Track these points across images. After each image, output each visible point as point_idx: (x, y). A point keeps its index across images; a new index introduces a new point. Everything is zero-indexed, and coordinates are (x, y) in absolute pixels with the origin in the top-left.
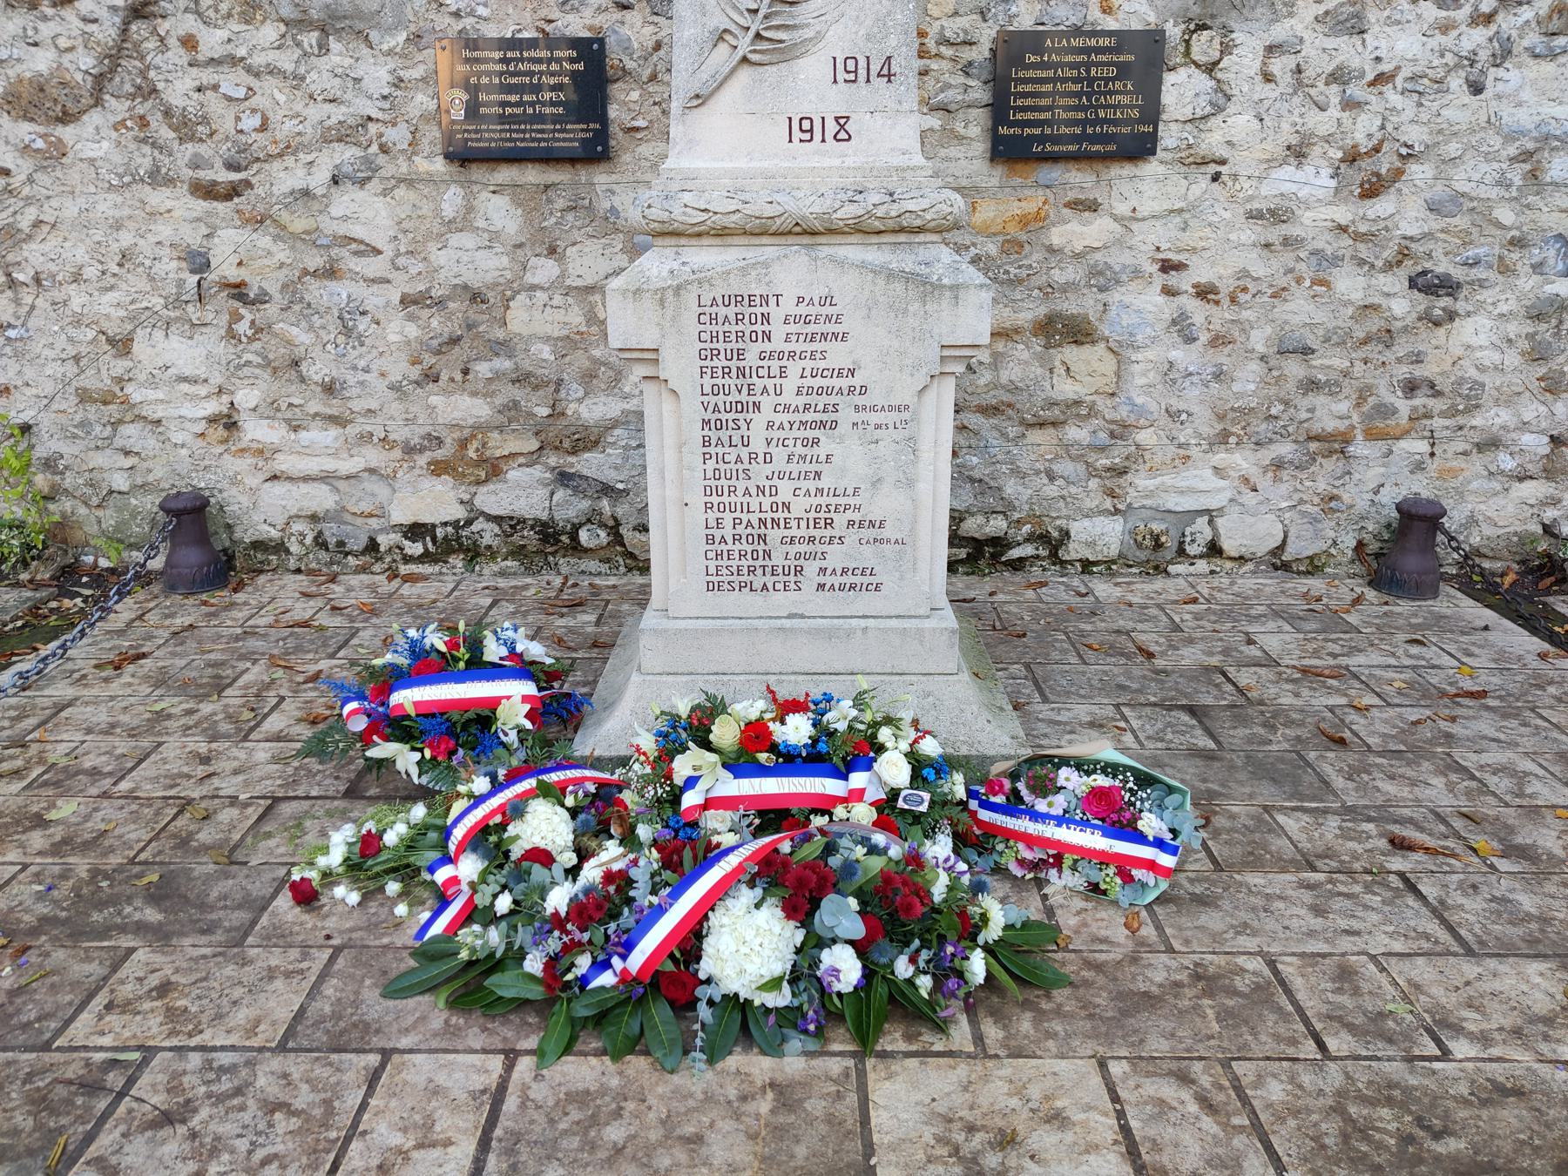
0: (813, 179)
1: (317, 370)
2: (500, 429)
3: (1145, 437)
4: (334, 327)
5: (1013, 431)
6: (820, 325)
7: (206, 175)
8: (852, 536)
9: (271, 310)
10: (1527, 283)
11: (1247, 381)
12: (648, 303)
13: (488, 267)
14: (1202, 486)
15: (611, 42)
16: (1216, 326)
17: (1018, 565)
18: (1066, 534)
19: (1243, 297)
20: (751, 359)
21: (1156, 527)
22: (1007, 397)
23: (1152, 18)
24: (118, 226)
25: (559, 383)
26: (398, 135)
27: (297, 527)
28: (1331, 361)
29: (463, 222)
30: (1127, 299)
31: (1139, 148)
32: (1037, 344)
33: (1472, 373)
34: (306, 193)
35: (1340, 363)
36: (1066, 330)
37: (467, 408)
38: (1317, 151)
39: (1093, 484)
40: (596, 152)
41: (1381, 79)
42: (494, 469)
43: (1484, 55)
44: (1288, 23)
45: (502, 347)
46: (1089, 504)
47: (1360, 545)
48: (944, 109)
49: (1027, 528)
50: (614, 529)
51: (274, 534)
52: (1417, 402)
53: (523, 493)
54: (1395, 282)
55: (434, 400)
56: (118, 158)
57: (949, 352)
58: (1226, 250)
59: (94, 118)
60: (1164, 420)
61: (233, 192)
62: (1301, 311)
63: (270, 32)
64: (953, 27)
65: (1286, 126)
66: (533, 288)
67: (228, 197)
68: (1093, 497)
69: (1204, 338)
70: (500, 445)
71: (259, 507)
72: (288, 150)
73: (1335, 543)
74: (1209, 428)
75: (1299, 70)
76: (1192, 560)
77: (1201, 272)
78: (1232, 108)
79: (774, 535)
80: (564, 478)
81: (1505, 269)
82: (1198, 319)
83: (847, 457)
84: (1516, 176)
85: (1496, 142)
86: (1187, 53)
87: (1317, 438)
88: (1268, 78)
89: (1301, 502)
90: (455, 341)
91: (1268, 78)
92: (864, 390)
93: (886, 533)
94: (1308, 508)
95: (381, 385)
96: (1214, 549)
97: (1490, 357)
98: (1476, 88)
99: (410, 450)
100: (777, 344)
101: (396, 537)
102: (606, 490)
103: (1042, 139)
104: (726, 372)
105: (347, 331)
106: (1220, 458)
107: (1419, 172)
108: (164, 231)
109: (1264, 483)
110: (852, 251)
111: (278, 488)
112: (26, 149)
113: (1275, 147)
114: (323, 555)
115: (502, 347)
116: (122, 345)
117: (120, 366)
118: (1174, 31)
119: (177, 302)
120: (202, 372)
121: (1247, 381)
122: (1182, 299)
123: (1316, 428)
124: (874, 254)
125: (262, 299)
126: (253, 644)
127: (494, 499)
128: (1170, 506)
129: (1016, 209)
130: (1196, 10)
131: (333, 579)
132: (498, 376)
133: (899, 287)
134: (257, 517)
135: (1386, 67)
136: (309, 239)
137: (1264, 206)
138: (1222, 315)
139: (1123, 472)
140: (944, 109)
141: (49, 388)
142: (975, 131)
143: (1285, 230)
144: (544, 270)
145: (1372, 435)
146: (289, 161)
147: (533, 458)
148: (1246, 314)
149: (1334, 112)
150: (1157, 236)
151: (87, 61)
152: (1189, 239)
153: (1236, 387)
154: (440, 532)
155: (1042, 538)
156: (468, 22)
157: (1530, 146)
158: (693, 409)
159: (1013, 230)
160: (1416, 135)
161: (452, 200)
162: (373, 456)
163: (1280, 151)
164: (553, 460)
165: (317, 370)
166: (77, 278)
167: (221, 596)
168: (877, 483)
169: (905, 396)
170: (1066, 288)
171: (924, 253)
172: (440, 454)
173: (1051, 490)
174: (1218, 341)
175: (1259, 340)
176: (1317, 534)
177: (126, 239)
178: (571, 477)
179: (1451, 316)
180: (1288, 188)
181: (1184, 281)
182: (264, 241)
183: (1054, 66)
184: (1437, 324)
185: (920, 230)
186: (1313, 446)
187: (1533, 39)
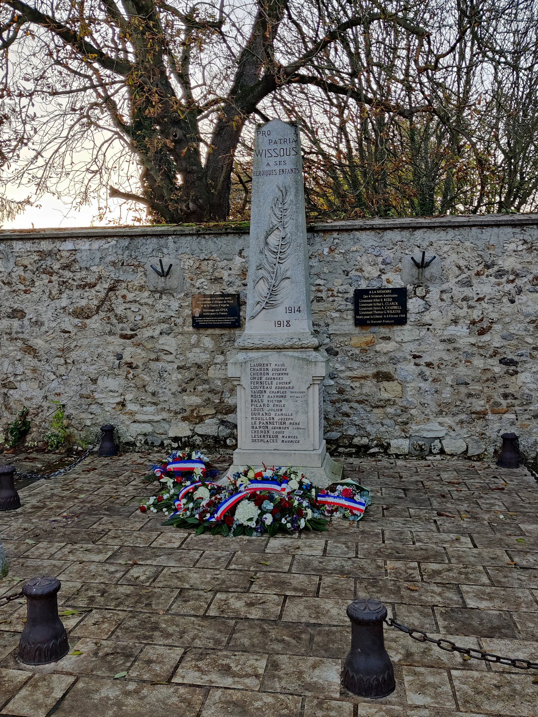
0: (280, 336)
1: (151, 389)
2: (204, 406)
3: (413, 411)
5: (369, 409)
6: (282, 371)
7: (124, 332)
9: (139, 370)
11: (447, 394)
12: (238, 366)
13: (204, 357)
14: (435, 429)
15: (241, 295)
16: (434, 375)
17: (373, 455)
18: (389, 444)
19: (442, 367)
20: (264, 379)
21: (420, 443)
22: (365, 398)
23: (403, 284)
24: (98, 347)
25: (223, 392)
26: (180, 321)
27: (140, 438)
28: (475, 387)
29: (196, 345)
30: (403, 367)
31: (402, 321)
32: (374, 381)
33: (527, 391)
34: (152, 337)
35: (478, 387)
36: (384, 377)
37: (195, 400)
38: (462, 321)
39: (397, 427)
41: (479, 300)
42: (201, 419)
43: (513, 292)
44: (447, 284)
45: (206, 382)
46: (396, 434)
47: (496, 452)
48: (339, 311)
49: (375, 442)
51: (132, 439)
52: (509, 401)
53: (210, 427)
54: (495, 361)
55: (185, 397)
56: (100, 328)
57: (314, 378)
58: (435, 352)
59: (96, 317)
60: (419, 406)
61: (132, 337)
62: (462, 370)
63: (146, 294)
64: (341, 289)
65: (450, 314)
66: (216, 364)
67: (130, 338)
68: (397, 431)
69: (430, 379)
70: (204, 412)
71: (130, 431)
72: (149, 325)
73: (486, 450)
74: (436, 409)
75: (452, 298)
76: (435, 455)
77: (427, 358)
78: (431, 309)
80: (223, 422)
83: (289, 405)
85: (522, 318)
86: (415, 293)
87: (474, 413)
88: (442, 300)
89: (472, 435)
90: (192, 380)
91: (442, 300)
92: (293, 388)
93: (300, 426)
94: (475, 437)
95: (169, 393)
96: (442, 452)
98: (512, 302)
99: (176, 413)
100: (270, 376)
101: (169, 441)
103: (370, 319)
104: (257, 383)
105: (161, 377)
106: (440, 419)
108: (111, 348)
109: (457, 428)
110: (290, 353)
111: (135, 425)
113: (447, 320)
114: (147, 447)
115: (206, 382)
116: (94, 381)
117: (93, 387)
118: (410, 288)
119: (112, 368)
120: (117, 389)
121: (447, 394)
122: (422, 367)
123: (474, 410)
124: (296, 354)
125: (137, 367)
126: (126, 468)
127: (201, 429)
128: (425, 435)
129: (364, 340)
130: (416, 281)
131: (149, 454)
132: (204, 390)
133: (301, 362)
135: (481, 296)
136: (152, 350)
137: (445, 338)
138: (436, 372)
139: (407, 424)
140: (339, 311)
141: (72, 394)
142: (350, 317)
143: (453, 345)
144: (220, 359)
145: (494, 412)
146: (149, 328)
147: (213, 416)
148: (443, 372)
149: (465, 309)
151: (96, 302)
152: (421, 348)
153: (443, 396)
154: (183, 440)
155: (380, 446)
156: (201, 290)
157: (534, 318)
159: (364, 346)
160: (494, 316)
161: (194, 339)
162: (165, 415)
163: (449, 322)
164: (219, 417)
165: (150, 389)
166: (85, 361)
167: (115, 457)
168: (297, 412)
169: (304, 389)
170: (382, 363)
171: (308, 354)
172: (185, 414)
173: (383, 429)
174: (435, 380)
175: (449, 380)
176: (479, 447)
177: (100, 350)
178: (225, 422)
179: (516, 372)
180: (452, 332)
181: (422, 361)
182: (139, 351)
183: (373, 298)
184: (512, 375)
185: (308, 348)
186: (474, 416)
187: (529, 286)
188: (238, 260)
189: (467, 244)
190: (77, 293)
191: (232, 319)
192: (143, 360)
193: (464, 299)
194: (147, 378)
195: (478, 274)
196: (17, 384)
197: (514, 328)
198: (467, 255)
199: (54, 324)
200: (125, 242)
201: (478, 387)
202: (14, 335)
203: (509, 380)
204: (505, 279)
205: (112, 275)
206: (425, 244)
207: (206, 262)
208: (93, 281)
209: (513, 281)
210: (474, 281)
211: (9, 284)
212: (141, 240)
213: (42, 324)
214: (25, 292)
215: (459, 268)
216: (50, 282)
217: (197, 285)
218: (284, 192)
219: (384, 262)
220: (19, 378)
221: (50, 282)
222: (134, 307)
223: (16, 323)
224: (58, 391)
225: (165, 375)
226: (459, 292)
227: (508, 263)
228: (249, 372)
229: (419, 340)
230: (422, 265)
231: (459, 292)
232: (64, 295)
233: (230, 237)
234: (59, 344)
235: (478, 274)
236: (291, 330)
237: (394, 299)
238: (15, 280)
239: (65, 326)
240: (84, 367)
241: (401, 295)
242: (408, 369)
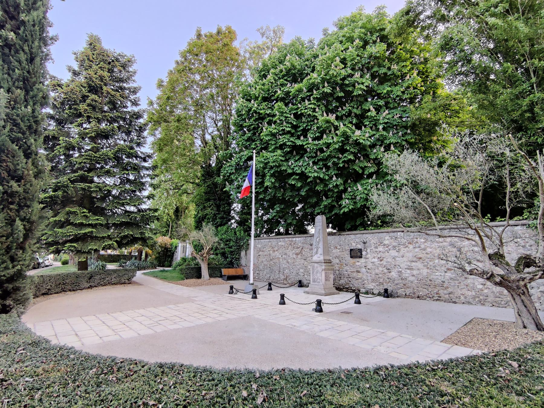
28: (381, 276)
54: (385, 268)
107: (385, 259)
201: (381, 276)
218: (320, 230)
234: (293, 261)
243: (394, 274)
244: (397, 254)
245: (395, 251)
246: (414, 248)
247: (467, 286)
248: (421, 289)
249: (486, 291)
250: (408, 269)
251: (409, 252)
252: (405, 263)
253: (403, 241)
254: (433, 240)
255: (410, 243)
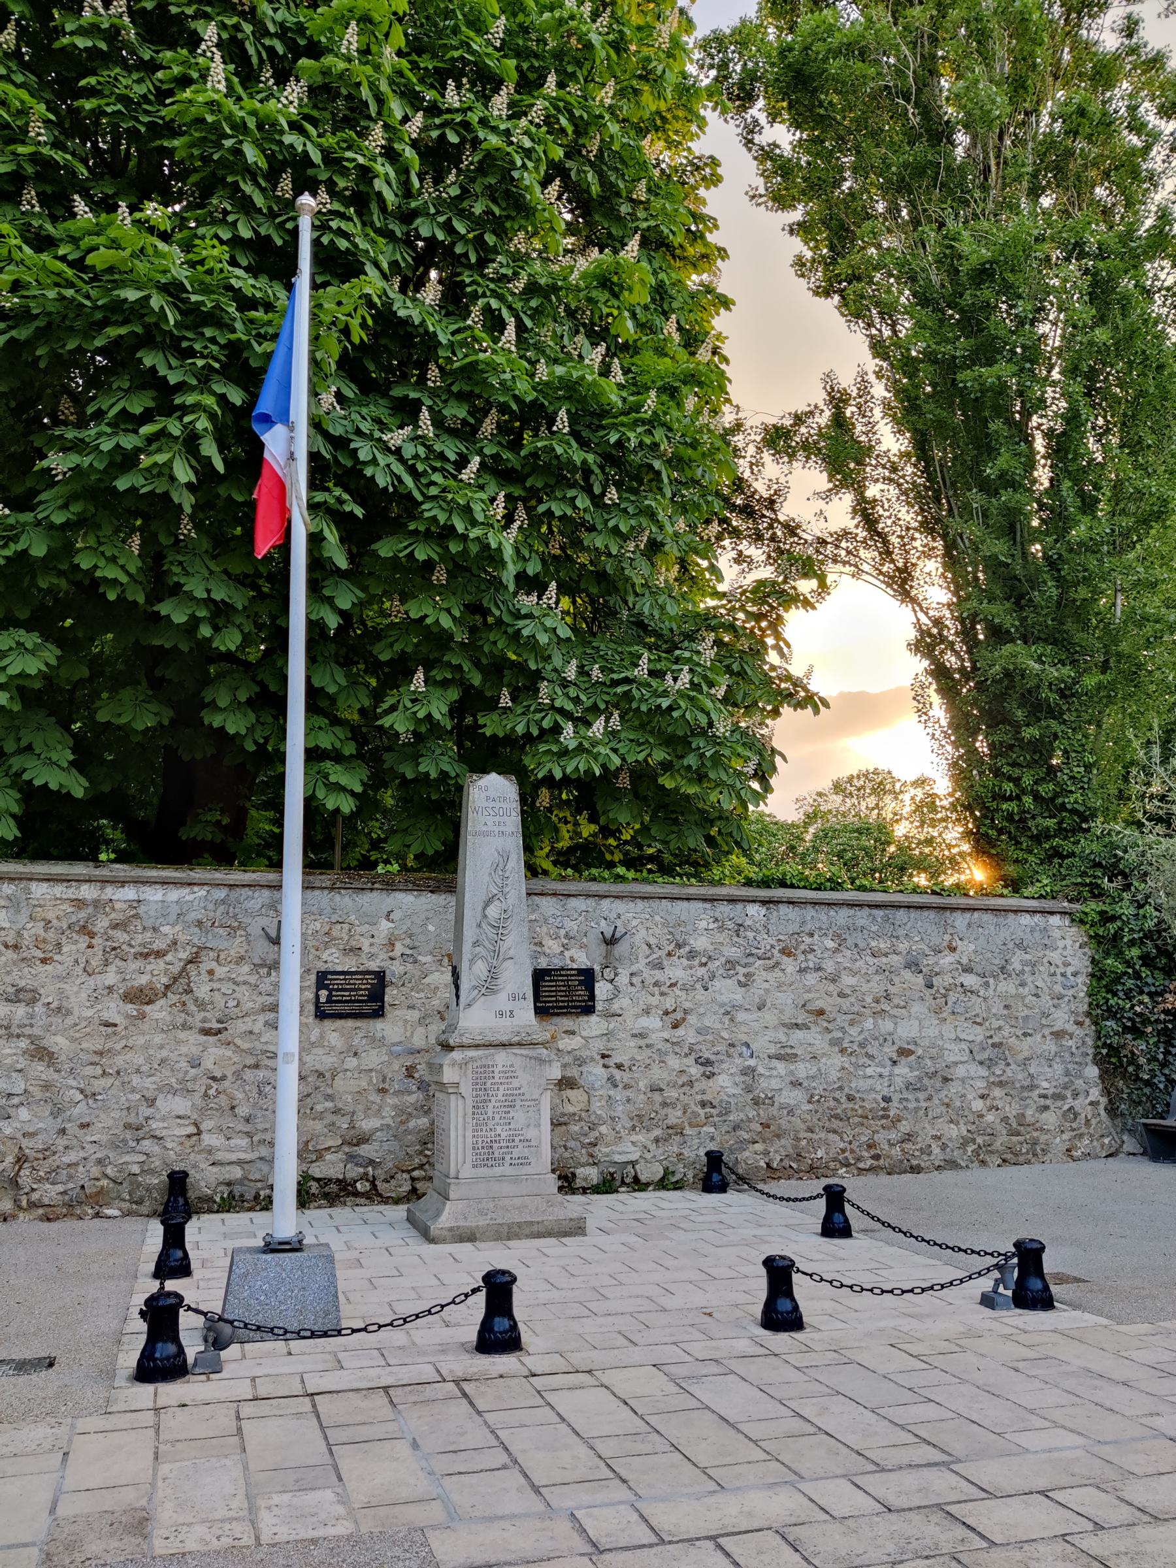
0: (504, 1029)
1: (243, 1111)
3: (603, 1129)
4: (255, 1090)
7: (207, 1025)
8: (521, 1145)
9: (226, 1083)
10: (738, 1061)
18: (574, 1175)
21: (612, 1170)
24: (162, 1047)
25: (354, 1113)
28: (672, 1094)
31: (589, 1010)
34: (251, 1032)
40: (379, 1013)
41: (672, 985)
42: (320, 1155)
46: (583, 1160)
50: (373, 1183)
54: (690, 1061)
56: (168, 1019)
59: (162, 1002)
61: (219, 1032)
62: (657, 1074)
63: (246, 968)
77: (617, 1058)
79: (495, 1145)
80: (351, 1157)
81: (729, 1056)
82: (618, 1078)
84: (726, 1019)
97: (732, 1091)
102: (371, 1162)
106: (634, 1138)
107: (692, 1019)
108: (184, 1049)
109: (653, 1147)
111: (215, 1169)
112: (128, 1016)
115: (329, 1097)
116: (151, 1103)
117: (149, 1112)
118: (597, 968)
120: (189, 1113)
125: (224, 1078)
134: (203, 1184)
141: (110, 1123)
144: (352, 1062)
146: (246, 1019)
149: (657, 997)
150: (599, 1045)
151: (165, 980)
152: (610, 1045)
158: (469, 1102)
160: (687, 1005)
164: (346, 1149)
166: (138, 1071)
173: (567, 1155)
174: (627, 1087)
177: (165, 1053)
187: (721, 971)
188: (385, 925)
189: (657, 918)
190: (134, 965)
191: (375, 1006)
192: (234, 1068)
193: (656, 984)
194: (240, 1096)
195: (669, 954)
196: (12, 1111)
197: (707, 1022)
198: (658, 931)
199: (90, 1013)
200: (221, 893)
202: (16, 1031)
203: (704, 1084)
204: (696, 962)
205: (196, 941)
206: (613, 915)
207: (339, 926)
208: (164, 946)
209: (705, 964)
210: (665, 963)
211: (16, 947)
212: (246, 892)
213: (69, 1012)
214: (44, 961)
215: (649, 946)
216: (90, 946)
217: (325, 957)
219: (567, 936)
220: (16, 1100)
221: (90, 946)
222: (226, 988)
223: (21, 1011)
224: (85, 1120)
225: (268, 1088)
226: (651, 975)
227: (700, 943)
228: (470, 1076)
229: (608, 1035)
230: (611, 941)
231: (651, 975)
232: (112, 969)
233: (375, 894)
235: (669, 954)
236: (515, 1021)
237: (581, 983)
238: (27, 940)
239: (107, 1016)
240: (136, 1080)
241: (588, 977)
242: (596, 1073)
243: (726, 1084)
244: (738, 996)
245: (731, 983)
246: (801, 971)
247: (948, 1105)
248: (822, 1135)
249: (990, 1118)
250: (779, 1057)
251: (783, 989)
252: (771, 1034)
253: (766, 941)
254: (862, 945)
255: (786, 952)
